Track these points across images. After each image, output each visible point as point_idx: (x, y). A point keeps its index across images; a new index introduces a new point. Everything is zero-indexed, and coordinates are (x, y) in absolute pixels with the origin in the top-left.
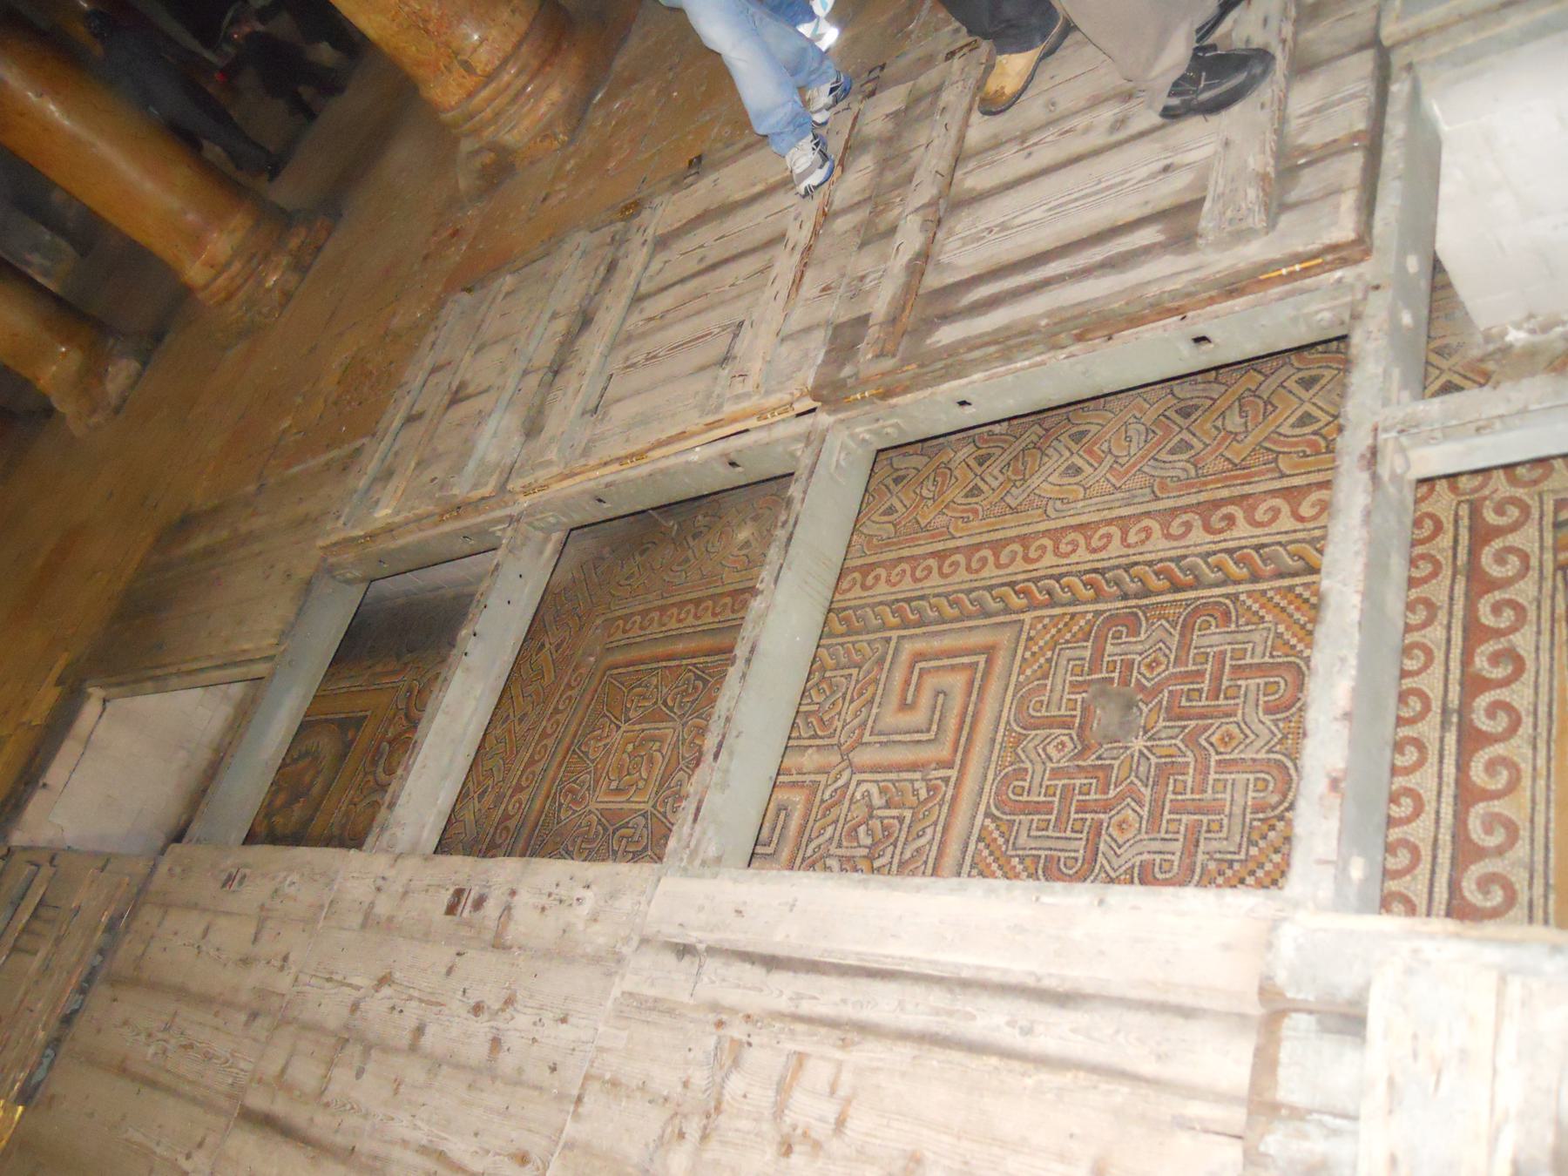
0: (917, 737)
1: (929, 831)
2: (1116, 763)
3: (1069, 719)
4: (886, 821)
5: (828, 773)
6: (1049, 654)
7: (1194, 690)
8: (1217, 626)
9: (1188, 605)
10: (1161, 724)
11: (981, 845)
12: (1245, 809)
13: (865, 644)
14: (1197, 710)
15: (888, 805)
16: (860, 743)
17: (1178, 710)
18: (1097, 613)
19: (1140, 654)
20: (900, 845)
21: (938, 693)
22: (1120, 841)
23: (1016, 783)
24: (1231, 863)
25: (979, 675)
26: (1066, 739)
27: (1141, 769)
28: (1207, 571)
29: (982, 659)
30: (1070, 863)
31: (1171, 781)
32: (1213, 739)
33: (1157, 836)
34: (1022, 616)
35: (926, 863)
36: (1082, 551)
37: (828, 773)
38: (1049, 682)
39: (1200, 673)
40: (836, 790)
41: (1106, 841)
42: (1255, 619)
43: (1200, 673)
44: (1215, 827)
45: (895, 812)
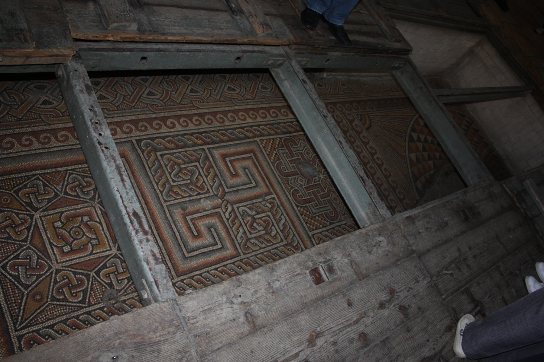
0: (248, 186)
1: (282, 216)
5: (220, 207)
11: (303, 216)
15: (258, 213)
16: (225, 193)
20: (275, 225)
23: (298, 194)
30: (331, 213)
35: (290, 227)
37: (220, 207)
45: (264, 215)
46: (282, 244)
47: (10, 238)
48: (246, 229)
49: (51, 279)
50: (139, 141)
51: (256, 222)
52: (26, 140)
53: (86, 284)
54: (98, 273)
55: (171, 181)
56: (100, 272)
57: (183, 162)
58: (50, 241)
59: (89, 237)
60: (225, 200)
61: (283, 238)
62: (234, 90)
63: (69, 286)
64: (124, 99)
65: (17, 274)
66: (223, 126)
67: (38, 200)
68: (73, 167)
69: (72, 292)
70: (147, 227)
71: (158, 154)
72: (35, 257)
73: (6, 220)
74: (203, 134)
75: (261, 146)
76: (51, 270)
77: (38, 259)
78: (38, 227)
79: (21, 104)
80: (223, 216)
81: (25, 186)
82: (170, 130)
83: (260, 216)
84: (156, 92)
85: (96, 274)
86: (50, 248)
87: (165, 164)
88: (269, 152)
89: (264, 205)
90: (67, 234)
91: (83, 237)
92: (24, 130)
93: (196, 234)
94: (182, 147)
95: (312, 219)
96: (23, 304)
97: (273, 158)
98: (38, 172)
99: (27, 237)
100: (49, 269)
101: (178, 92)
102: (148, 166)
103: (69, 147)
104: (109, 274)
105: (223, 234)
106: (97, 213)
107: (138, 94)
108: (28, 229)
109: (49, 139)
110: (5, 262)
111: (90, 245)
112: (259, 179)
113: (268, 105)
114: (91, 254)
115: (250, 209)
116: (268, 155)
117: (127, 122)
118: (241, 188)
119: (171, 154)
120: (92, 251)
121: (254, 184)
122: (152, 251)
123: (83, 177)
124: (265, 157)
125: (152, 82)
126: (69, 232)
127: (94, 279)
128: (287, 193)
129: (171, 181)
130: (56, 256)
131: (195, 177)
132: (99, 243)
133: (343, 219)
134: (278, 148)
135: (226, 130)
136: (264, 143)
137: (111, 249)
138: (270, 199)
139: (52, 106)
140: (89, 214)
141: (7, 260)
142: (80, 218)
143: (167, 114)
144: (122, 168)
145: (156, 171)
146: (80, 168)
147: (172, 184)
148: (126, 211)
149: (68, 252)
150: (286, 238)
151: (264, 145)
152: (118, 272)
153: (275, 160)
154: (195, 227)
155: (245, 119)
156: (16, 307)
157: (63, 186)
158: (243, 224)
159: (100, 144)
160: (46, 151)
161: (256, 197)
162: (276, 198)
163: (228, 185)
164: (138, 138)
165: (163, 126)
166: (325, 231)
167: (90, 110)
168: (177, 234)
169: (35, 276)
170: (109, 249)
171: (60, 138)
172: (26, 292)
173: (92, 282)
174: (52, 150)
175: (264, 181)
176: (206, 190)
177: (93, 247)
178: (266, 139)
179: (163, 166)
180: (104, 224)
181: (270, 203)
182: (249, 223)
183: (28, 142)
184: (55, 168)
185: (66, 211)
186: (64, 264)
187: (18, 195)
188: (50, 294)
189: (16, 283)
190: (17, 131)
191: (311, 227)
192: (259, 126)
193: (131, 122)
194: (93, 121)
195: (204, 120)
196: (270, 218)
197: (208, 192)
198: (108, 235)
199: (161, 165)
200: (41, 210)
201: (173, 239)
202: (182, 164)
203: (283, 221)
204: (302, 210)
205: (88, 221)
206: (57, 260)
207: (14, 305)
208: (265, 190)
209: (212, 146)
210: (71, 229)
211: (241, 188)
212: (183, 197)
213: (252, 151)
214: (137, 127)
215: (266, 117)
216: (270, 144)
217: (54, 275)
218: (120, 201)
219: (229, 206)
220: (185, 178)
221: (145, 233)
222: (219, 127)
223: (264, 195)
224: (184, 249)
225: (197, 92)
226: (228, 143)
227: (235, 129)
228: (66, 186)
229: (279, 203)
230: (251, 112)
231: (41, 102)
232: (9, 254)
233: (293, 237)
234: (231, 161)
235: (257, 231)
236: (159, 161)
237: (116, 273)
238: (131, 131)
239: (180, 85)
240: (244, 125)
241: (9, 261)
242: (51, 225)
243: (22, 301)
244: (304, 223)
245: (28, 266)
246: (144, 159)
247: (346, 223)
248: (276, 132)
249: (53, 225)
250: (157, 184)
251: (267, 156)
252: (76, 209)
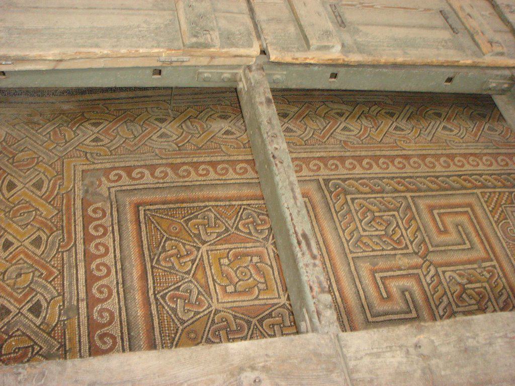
0: (461, 247)
1: (504, 291)
4: (476, 290)
15: (470, 282)
16: (428, 252)
20: (493, 300)
21: (457, 226)
45: (478, 285)
47: (173, 268)
48: (451, 300)
49: (209, 319)
50: (327, 181)
52: (203, 170)
53: (246, 332)
54: (261, 321)
55: (360, 229)
56: (263, 321)
57: (379, 210)
58: (213, 278)
59: (256, 280)
60: (427, 260)
62: (451, 131)
63: (227, 330)
64: (313, 134)
65: (175, 306)
66: (433, 172)
67: (207, 233)
68: (248, 202)
69: (230, 337)
70: (315, 251)
71: (349, 197)
72: (195, 292)
73: (172, 249)
74: (407, 180)
75: (482, 200)
76: (210, 309)
77: (198, 294)
78: (203, 261)
79: (203, 133)
80: (423, 281)
81: (196, 217)
82: (365, 172)
83: (473, 286)
84: (352, 128)
85: (259, 323)
86: (213, 285)
87: (355, 210)
88: (493, 208)
90: (233, 274)
91: (250, 278)
92: (202, 159)
93: (385, 295)
94: (378, 193)
96: (176, 339)
97: (497, 216)
98: (211, 203)
99: (190, 270)
100: (208, 308)
101: (379, 129)
102: (335, 210)
103: (247, 181)
104: (273, 325)
106: (269, 255)
107: (331, 128)
108: (193, 261)
109: (227, 170)
110: (165, 292)
111: (256, 288)
112: (476, 240)
113: (495, 151)
114: (257, 298)
115: (460, 275)
116: (491, 212)
117: (314, 158)
118: (450, 248)
119: (363, 198)
120: (258, 296)
121: (468, 246)
122: (318, 278)
123: (259, 214)
124: (486, 214)
125: (348, 117)
126: (236, 272)
127: (255, 327)
129: (360, 229)
130: (217, 295)
131: (392, 229)
132: (267, 289)
134: (505, 204)
135: (437, 177)
136: (487, 196)
137: (279, 298)
138: (488, 267)
139: (234, 136)
140: (260, 256)
141: (167, 291)
142: (250, 258)
143: (363, 153)
144: (295, 185)
145: (344, 216)
146: (256, 204)
147: (362, 233)
148: (295, 230)
149: (231, 293)
151: (486, 199)
152: (283, 325)
153: (501, 219)
154: (385, 287)
155: (463, 166)
156: (169, 342)
157: (235, 221)
159: (274, 157)
160: (222, 182)
161: (470, 262)
163: (433, 244)
164: (326, 177)
165: (358, 166)
167: (269, 123)
168: (361, 292)
169: (193, 313)
170: (277, 296)
171: (238, 170)
172: (181, 327)
173: (253, 331)
174: (229, 182)
175: (482, 242)
176: (404, 245)
177: (259, 292)
178: (490, 193)
179: (353, 211)
181: (489, 272)
182: (456, 293)
183: (205, 172)
184: (229, 201)
185: (235, 248)
186: (225, 305)
187: (187, 225)
188: (206, 335)
189: (173, 316)
190: (195, 160)
192: (481, 175)
193: (319, 158)
194: (269, 134)
195: (409, 164)
197: (406, 247)
198: (278, 281)
199: (351, 211)
200: (209, 243)
201: (356, 298)
202: (377, 212)
203: (504, 297)
205: (257, 263)
206: (218, 299)
207: (168, 338)
208: (483, 254)
209: (417, 194)
210: (237, 269)
212: (373, 250)
213: (470, 205)
214: (326, 165)
215: (491, 165)
216: (495, 199)
217: (212, 315)
218: (289, 219)
220: (379, 229)
221: (314, 257)
222: (428, 172)
224: (367, 311)
225: (403, 130)
226: (437, 193)
227: (448, 177)
228: (239, 222)
230: (471, 158)
231: (223, 131)
232: (170, 284)
234: (440, 215)
235: (467, 304)
236: (349, 206)
237: (282, 325)
238: (319, 169)
239: (382, 122)
240: (460, 173)
241: (169, 292)
242: (218, 261)
243: (176, 336)
245: (187, 301)
246: (330, 202)
248: (503, 184)
249: (219, 261)
250: (344, 231)
251: (489, 213)
252: (246, 248)
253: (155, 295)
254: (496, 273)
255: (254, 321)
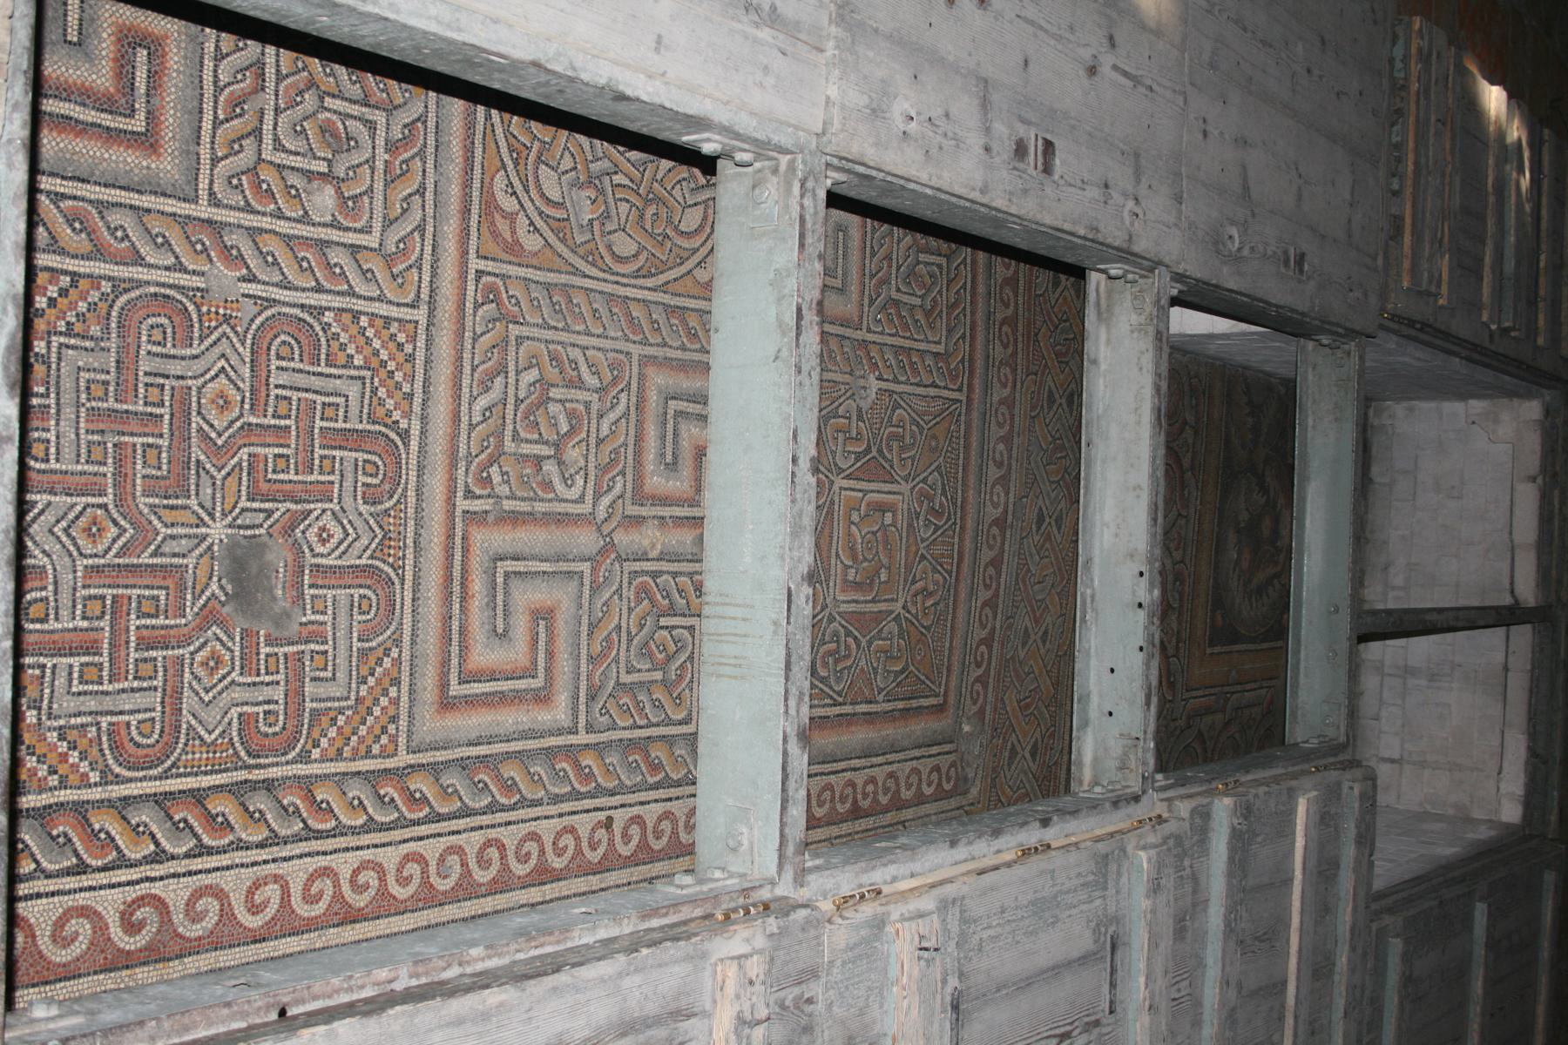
0: (520, 566)
1: (477, 418)
2: (243, 503)
3: (320, 582)
6: (363, 692)
7: (149, 616)
8: (128, 724)
9: (174, 765)
10: (190, 561)
11: (406, 388)
12: (58, 411)
13: (621, 723)
14: (139, 581)
15: (538, 461)
16: (595, 560)
17: (169, 582)
18: (304, 757)
19: (233, 682)
20: (511, 400)
22: (223, 379)
23: (375, 481)
24: (69, 333)
25: (455, 661)
26: (319, 549)
27: (209, 491)
28: (155, 829)
29: (455, 689)
30: (285, 351)
31: (165, 467)
32: (114, 531)
33: (175, 383)
34: (412, 759)
35: (473, 370)
36: (345, 873)
38: (356, 644)
39: (145, 644)
40: (610, 489)
41: (243, 380)
42: (72, 735)
43: (145, 644)
44: (97, 391)
45: (527, 449)
46: (525, 331)
51: (558, 434)
54: (868, 450)
61: (512, 349)
89: (508, 482)
95: (383, 364)
105: (651, 431)
114: (865, 492)
118: (545, 567)
128: (412, 499)
133: (250, 308)
150: (506, 340)
158: (593, 441)
162: (460, 494)
166: (360, 297)
178: (368, 754)
180: (833, 551)
182: (577, 440)
191: (401, 338)
196: (515, 430)
204: (396, 415)
208: (478, 536)
211: (545, 567)
219: (601, 513)
223: (491, 518)
229: (461, 471)
233: (483, 334)
235: (567, 405)
244: (420, 361)
247: (243, 279)
253: (955, 523)
254: (471, 476)
255: (874, 453)
